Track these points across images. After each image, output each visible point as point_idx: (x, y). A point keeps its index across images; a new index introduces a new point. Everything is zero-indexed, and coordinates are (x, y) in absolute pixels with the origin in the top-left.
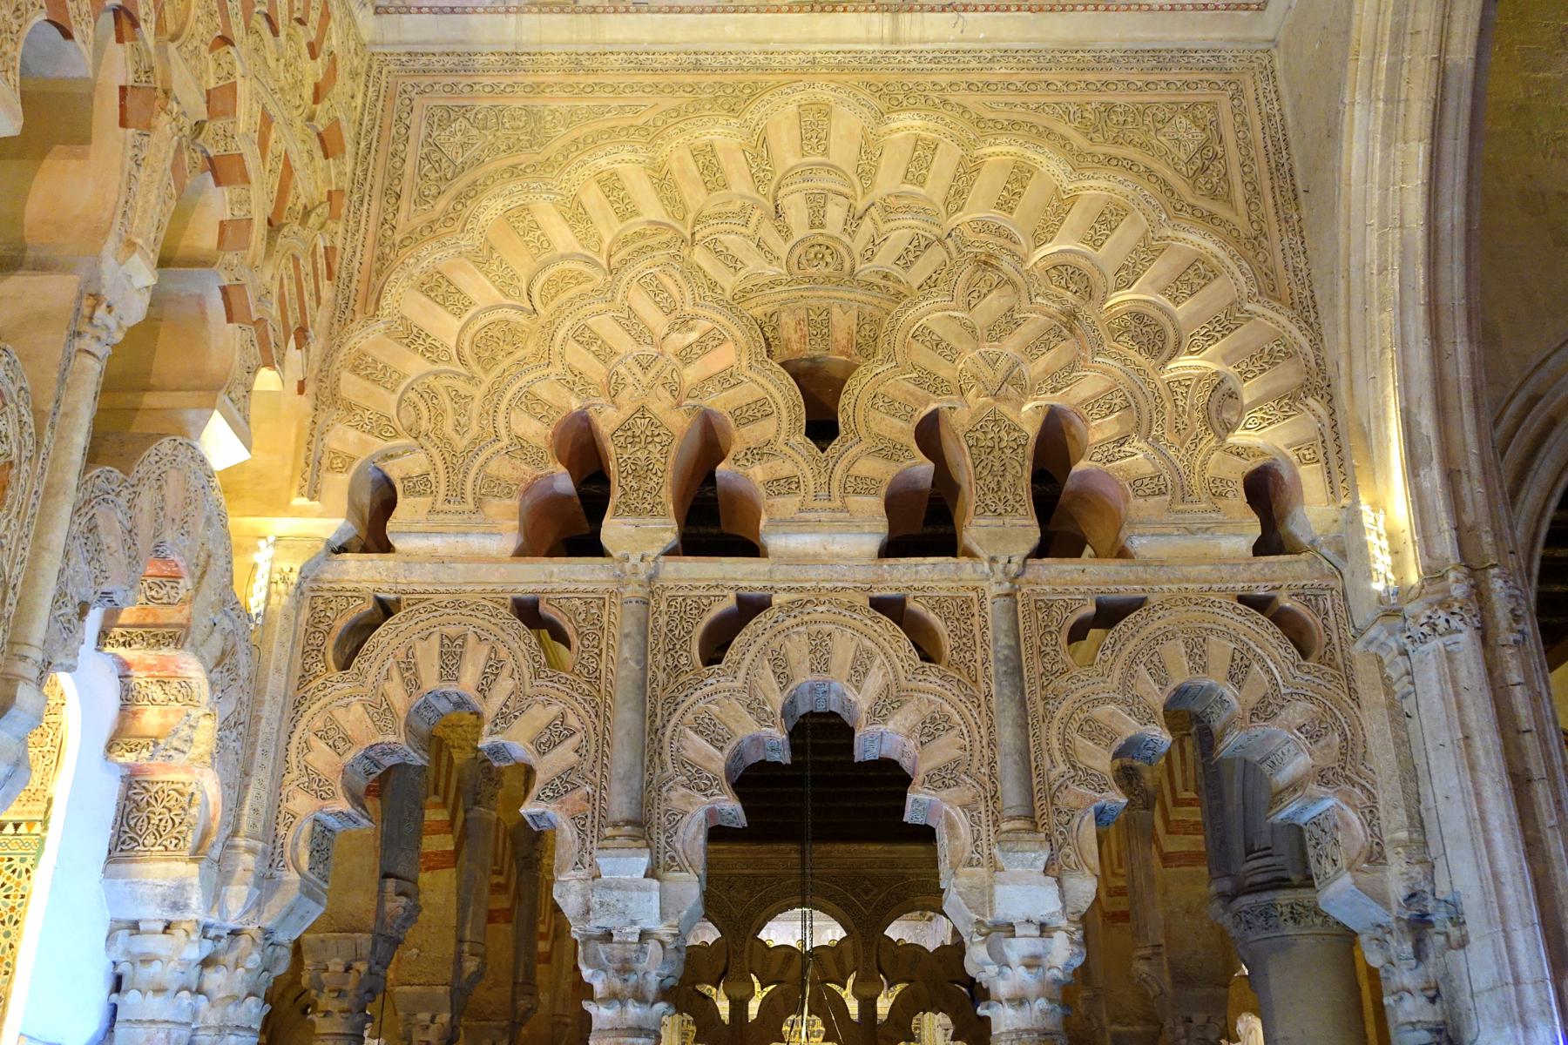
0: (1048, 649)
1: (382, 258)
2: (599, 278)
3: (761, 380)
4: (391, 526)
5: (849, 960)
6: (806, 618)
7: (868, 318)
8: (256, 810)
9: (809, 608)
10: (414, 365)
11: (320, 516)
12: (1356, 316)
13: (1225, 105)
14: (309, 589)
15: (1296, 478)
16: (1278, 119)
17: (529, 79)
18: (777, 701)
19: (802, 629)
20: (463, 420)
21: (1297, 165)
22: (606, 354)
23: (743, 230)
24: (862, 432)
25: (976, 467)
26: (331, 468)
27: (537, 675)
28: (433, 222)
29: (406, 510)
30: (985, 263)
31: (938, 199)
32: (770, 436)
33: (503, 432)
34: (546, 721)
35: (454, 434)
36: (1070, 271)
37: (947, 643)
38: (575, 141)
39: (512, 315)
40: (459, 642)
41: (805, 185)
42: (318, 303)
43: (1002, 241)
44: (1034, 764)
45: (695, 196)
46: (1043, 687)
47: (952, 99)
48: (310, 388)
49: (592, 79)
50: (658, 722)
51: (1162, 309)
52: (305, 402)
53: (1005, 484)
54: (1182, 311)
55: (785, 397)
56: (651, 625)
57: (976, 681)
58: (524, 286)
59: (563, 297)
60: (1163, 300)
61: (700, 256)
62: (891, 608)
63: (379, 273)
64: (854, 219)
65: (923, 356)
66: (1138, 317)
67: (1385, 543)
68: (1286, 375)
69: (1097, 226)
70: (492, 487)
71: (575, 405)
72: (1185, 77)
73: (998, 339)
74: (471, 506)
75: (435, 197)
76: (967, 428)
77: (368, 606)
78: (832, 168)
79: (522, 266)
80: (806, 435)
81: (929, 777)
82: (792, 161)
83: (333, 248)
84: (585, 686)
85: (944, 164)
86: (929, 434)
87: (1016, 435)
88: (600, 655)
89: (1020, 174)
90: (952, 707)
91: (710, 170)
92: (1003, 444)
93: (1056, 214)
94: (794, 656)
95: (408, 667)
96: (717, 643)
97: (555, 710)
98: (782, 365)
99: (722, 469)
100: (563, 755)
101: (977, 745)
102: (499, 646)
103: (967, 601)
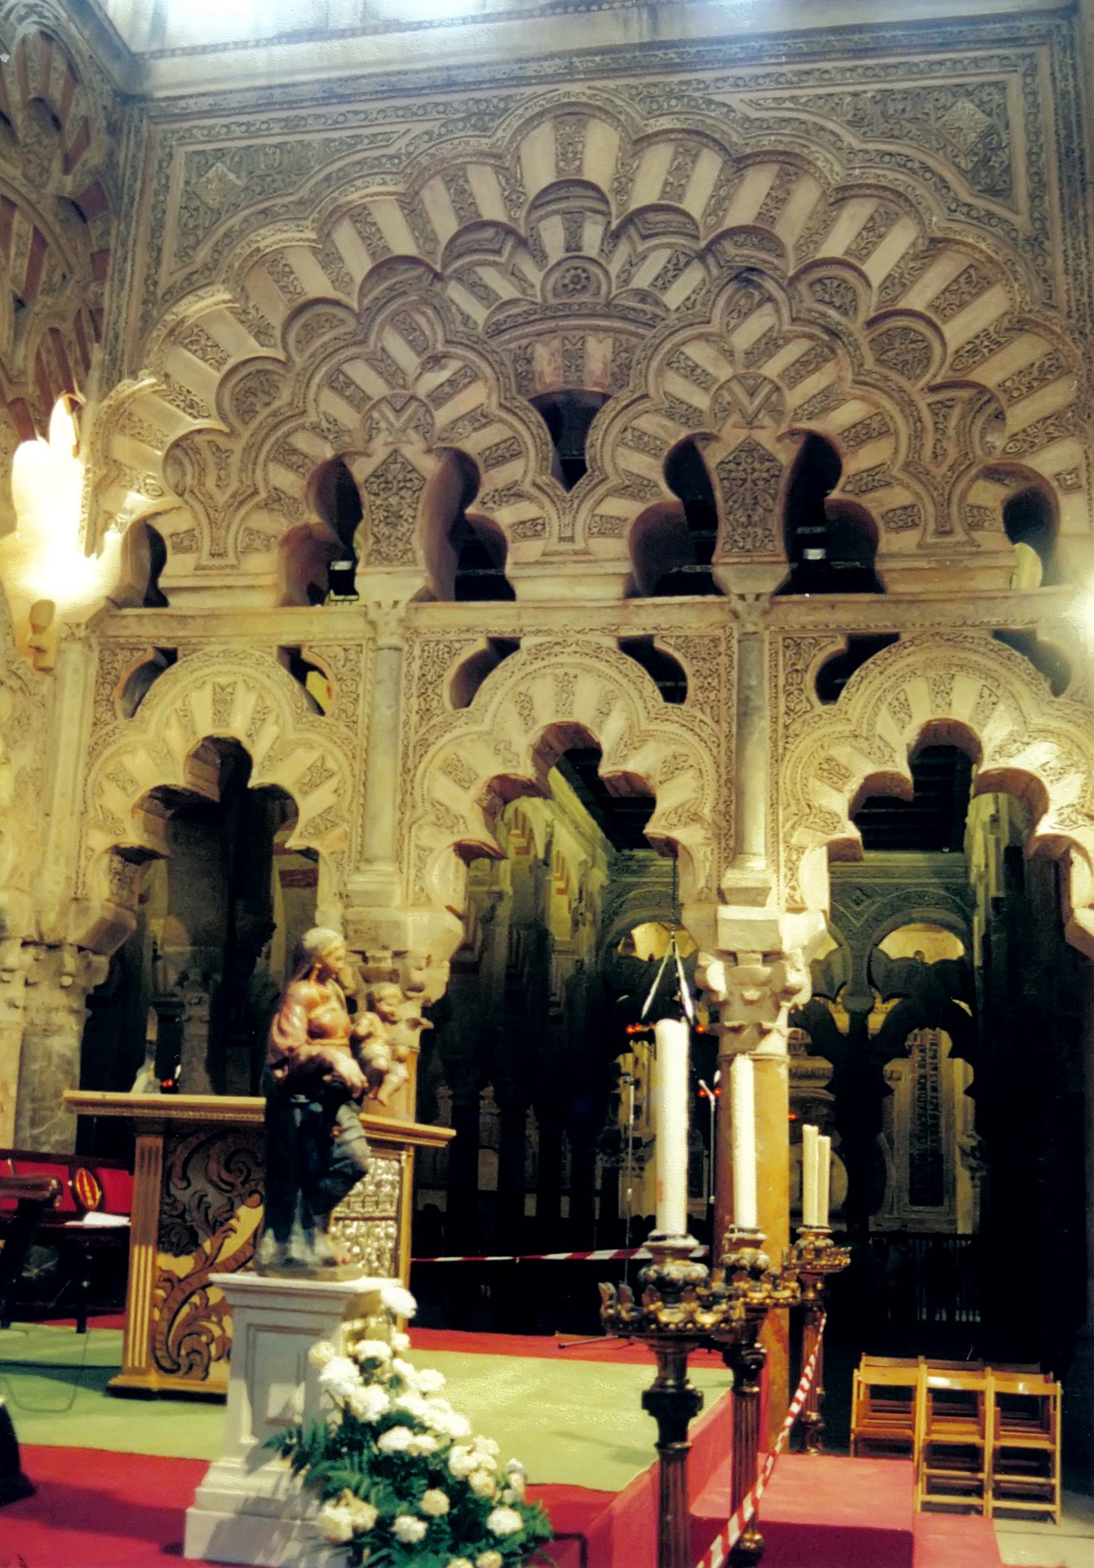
0: (792, 689)
4: (163, 582)
7: (625, 346)
9: (557, 649)
15: (1057, 506)
16: (1072, 96)
19: (548, 671)
20: (223, 473)
21: (1088, 152)
22: (359, 400)
23: (497, 259)
24: (609, 469)
25: (726, 502)
28: (192, 274)
32: (518, 476)
34: (308, 764)
35: (215, 491)
36: (836, 284)
38: (328, 178)
40: (229, 690)
41: (563, 205)
42: (87, 366)
43: (764, 256)
46: (786, 727)
49: (345, 108)
50: (410, 765)
53: (755, 518)
56: (404, 669)
58: (278, 333)
61: (455, 292)
64: (614, 237)
65: (677, 385)
69: (864, 233)
71: (329, 453)
75: (194, 248)
76: (718, 460)
77: (150, 655)
83: (100, 311)
84: (345, 730)
87: (767, 464)
88: (356, 700)
91: (463, 198)
92: (756, 475)
94: (538, 703)
95: (185, 716)
97: (313, 756)
99: (471, 510)
102: (264, 694)
103: (715, 641)
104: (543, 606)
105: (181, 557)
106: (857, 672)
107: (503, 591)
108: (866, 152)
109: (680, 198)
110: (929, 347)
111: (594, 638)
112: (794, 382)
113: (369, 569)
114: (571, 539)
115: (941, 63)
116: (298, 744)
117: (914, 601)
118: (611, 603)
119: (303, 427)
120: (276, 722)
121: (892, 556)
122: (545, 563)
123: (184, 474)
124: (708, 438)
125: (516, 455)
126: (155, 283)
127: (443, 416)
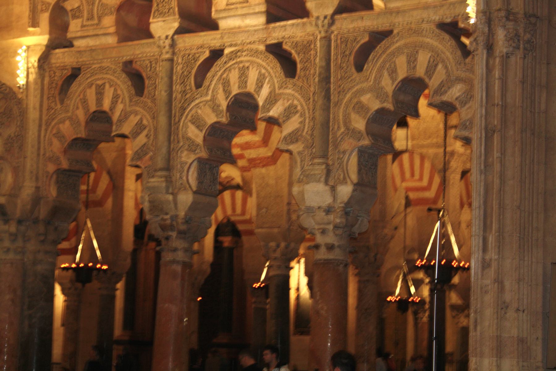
4: (69, 35)
6: (238, 60)
8: (31, 172)
9: (239, 54)
11: (40, 34)
18: (224, 104)
26: (42, 10)
27: (131, 101)
29: (74, 27)
44: (331, 129)
50: (177, 119)
56: (175, 70)
57: (310, 86)
74: (96, 21)
90: (298, 101)
95: (84, 101)
97: (138, 117)
100: (141, 139)
101: (307, 121)
103: (310, 43)
105: (75, 21)
106: (372, 53)
107: (213, 26)
111: (254, 47)
113: (155, 20)
116: (131, 113)
118: (261, 27)
120: (122, 102)
122: (229, 9)
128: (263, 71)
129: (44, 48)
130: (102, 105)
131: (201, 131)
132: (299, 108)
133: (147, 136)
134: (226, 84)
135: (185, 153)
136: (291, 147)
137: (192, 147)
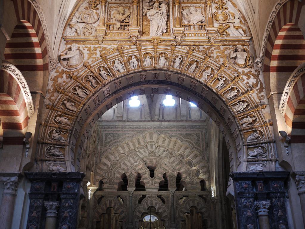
1: (101, 154)
2: (126, 156)
3: (145, 169)
5: (158, 224)
10: (105, 168)
12: (212, 164)
13: (200, 133)
14: (94, 195)
17: (117, 129)
18: (147, 208)
22: (127, 166)
24: (157, 176)
26: (96, 181)
29: (105, 186)
30: (171, 154)
31: (166, 146)
33: (115, 176)
37: (166, 201)
38: (123, 138)
39: (116, 161)
43: (173, 151)
45: (137, 145)
47: (168, 132)
48: (94, 171)
51: (191, 160)
52: (93, 173)
54: (194, 161)
55: (148, 171)
59: (122, 159)
60: (192, 159)
61: (138, 153)
62: (160, 197)
63: (101, 156)
65: (164, 166)
66: (189, 161)
67: (213, 192)
68: (205, 169)
70: (115, 183)
71: (124, 172)
72: (196, 129)
73: (173, 164)
74: (112, 185)
77: (101, 197)
78: (153, 141)
79: (117, 155)
80: (150, 176)
81: (164, 217)
82: (149, 141)
85: (167, 140)
86: (164, 176)
89: (176, 142)
93: (180, 148)
95: (106, 204)
96: (140, 201)
97: (122, 209)
98: (147, 167)
100: (123, 215)
103: (168, 196)
104: (149, 192)
107: (144, 190)
108: (184, 140)
109: (164, 144)
110: (191, 163)
112: (177, 167)
114: (153, 184)
115: (192, 130)
117: (190, 192)
119: (120, 169)
121: (188, 187)
123: (106, 174)
124: (167, 173)
125: (146, 174)
126: (102, 150)
127: (137, 168)
128: (157, 201)
129: (96, 190)
130: (111, 205)
131: (141, 214)
132: (167, 210)
133: (125, 214)
134: (147, 204)
135: (136, 219)
136: (165, 219)
137: (138, 217)
